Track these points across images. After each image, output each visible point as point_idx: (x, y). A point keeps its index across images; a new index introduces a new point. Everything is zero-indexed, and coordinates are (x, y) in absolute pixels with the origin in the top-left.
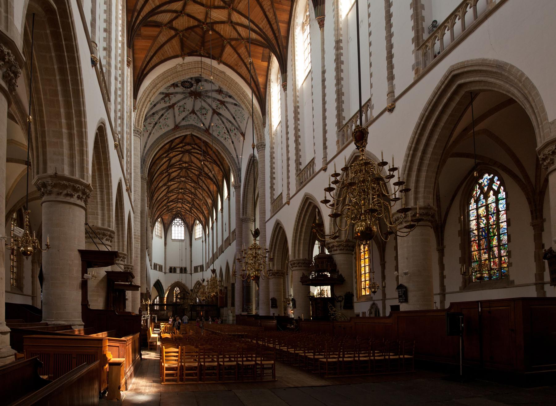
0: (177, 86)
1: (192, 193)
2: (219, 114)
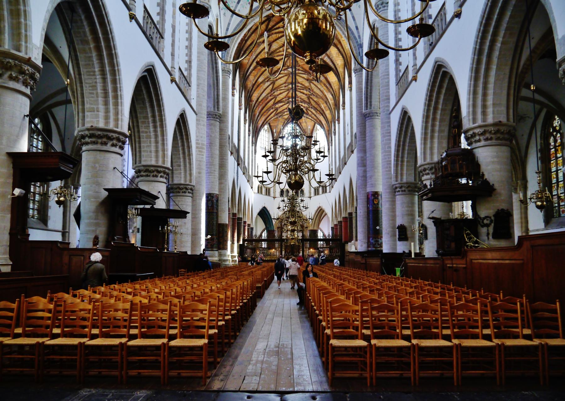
1: (305, 88)
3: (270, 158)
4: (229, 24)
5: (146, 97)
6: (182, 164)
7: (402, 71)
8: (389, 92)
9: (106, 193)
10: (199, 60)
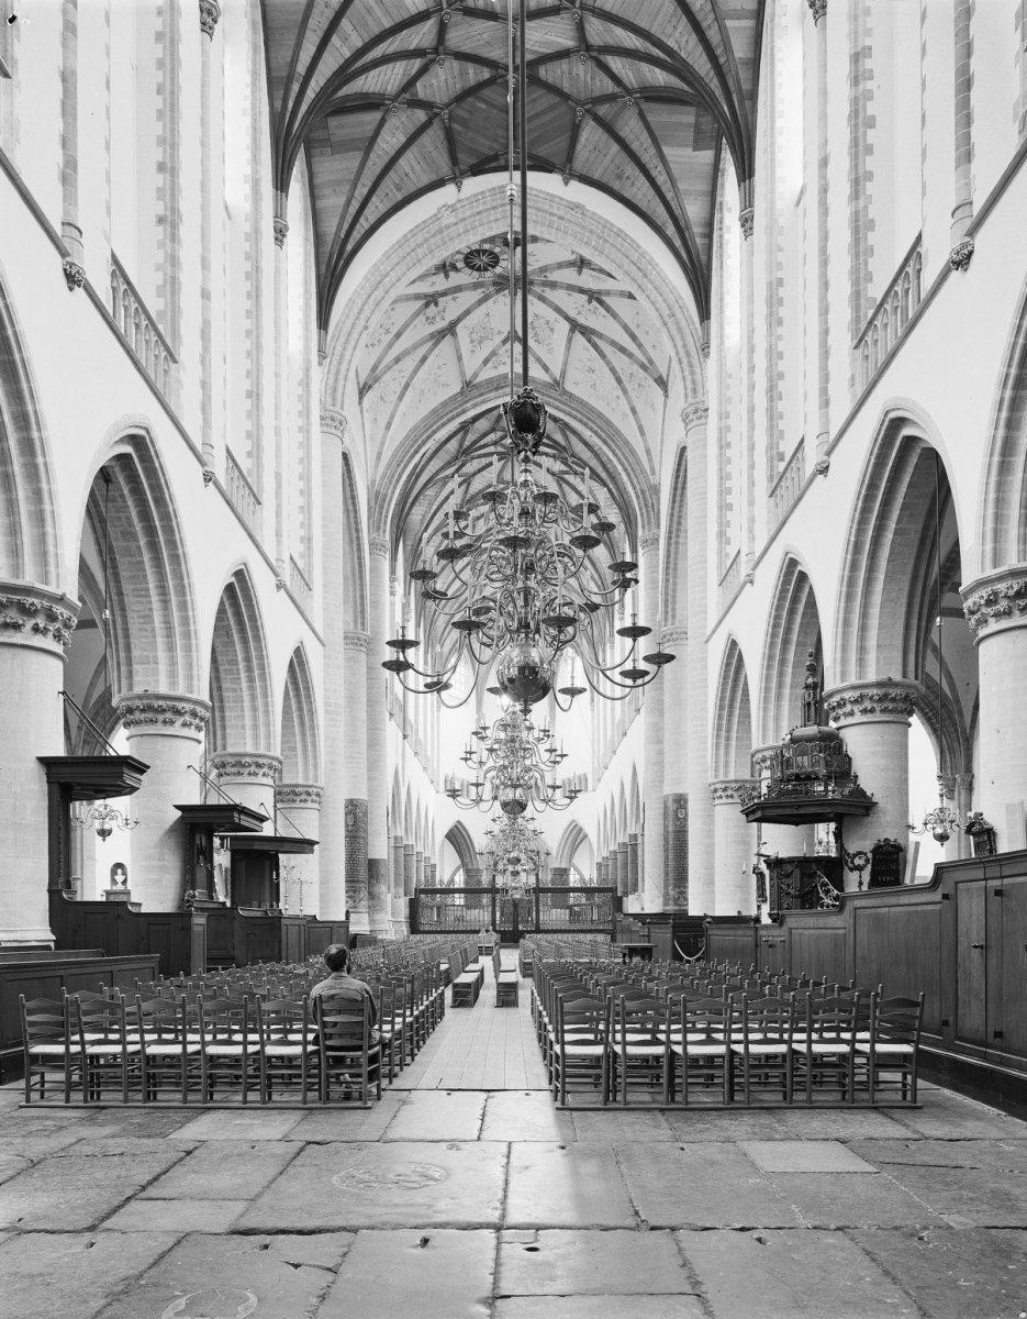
2: (587, 332)
5: (232, 623)
6: (299, 745)
10: (325, 534)
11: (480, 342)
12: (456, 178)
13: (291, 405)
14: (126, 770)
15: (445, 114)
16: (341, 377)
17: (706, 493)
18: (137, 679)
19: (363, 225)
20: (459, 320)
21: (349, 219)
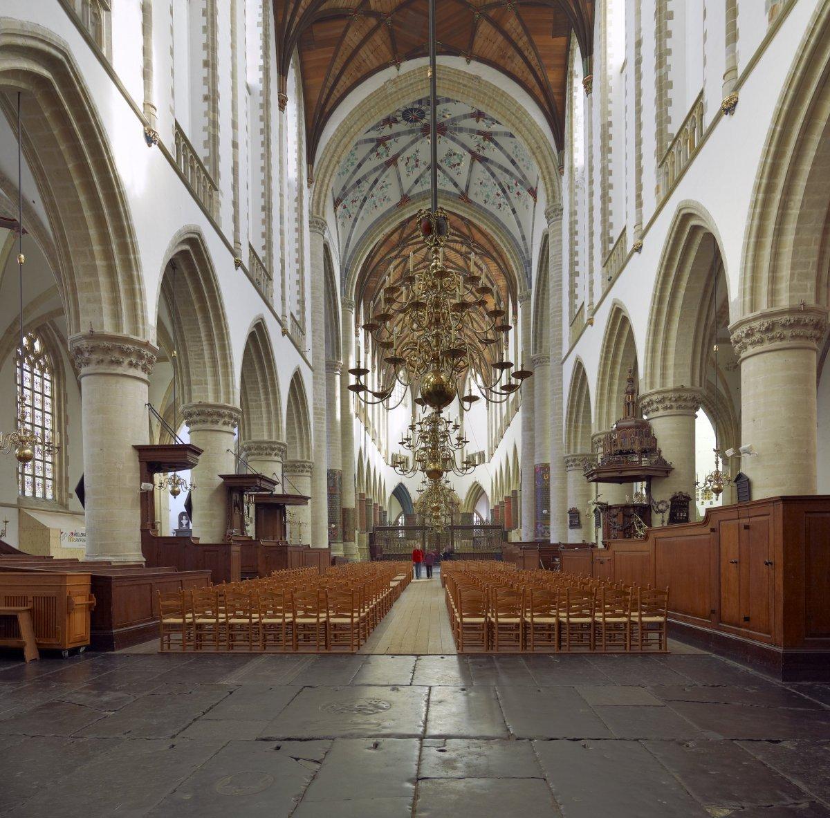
0: (396, 121)
2: (483, 160)
3: (407, 444)
4: (349, 238)
6: (297, 435)
7: (579, 307)
8: (561, 335)
9: (222, 480)
10: (313, 298)
11: (412, 168)
12: (397, 63)
13: (290, 215)
14: (188, 453)
15: (389, 20)
16: (323, 195)
17: (561, 265)
18: (194, 395)
19: (336, 94)
20: (398, 155)
21: (327, 91)
